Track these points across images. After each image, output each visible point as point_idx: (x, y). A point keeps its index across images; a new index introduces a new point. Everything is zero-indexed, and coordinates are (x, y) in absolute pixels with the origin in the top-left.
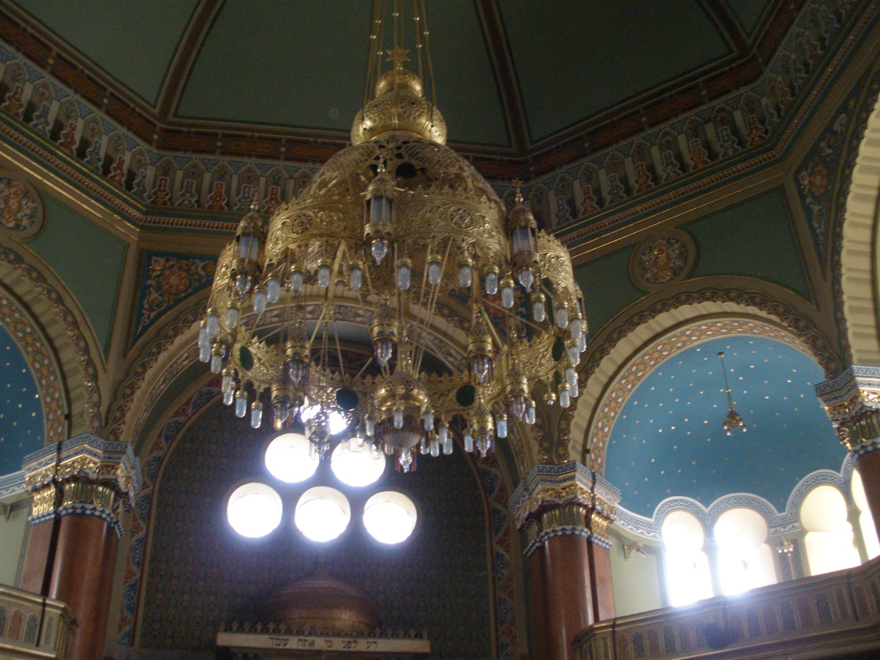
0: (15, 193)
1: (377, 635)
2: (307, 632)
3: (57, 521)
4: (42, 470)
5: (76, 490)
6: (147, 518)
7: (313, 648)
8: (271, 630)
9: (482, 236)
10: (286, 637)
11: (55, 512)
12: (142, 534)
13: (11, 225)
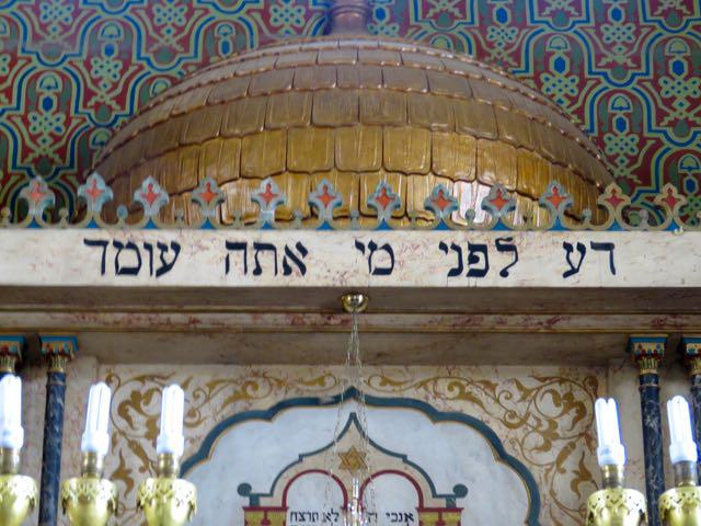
1: (615, 213)
7: (295, 280)
8: (94, 208)
10: (168, 236)
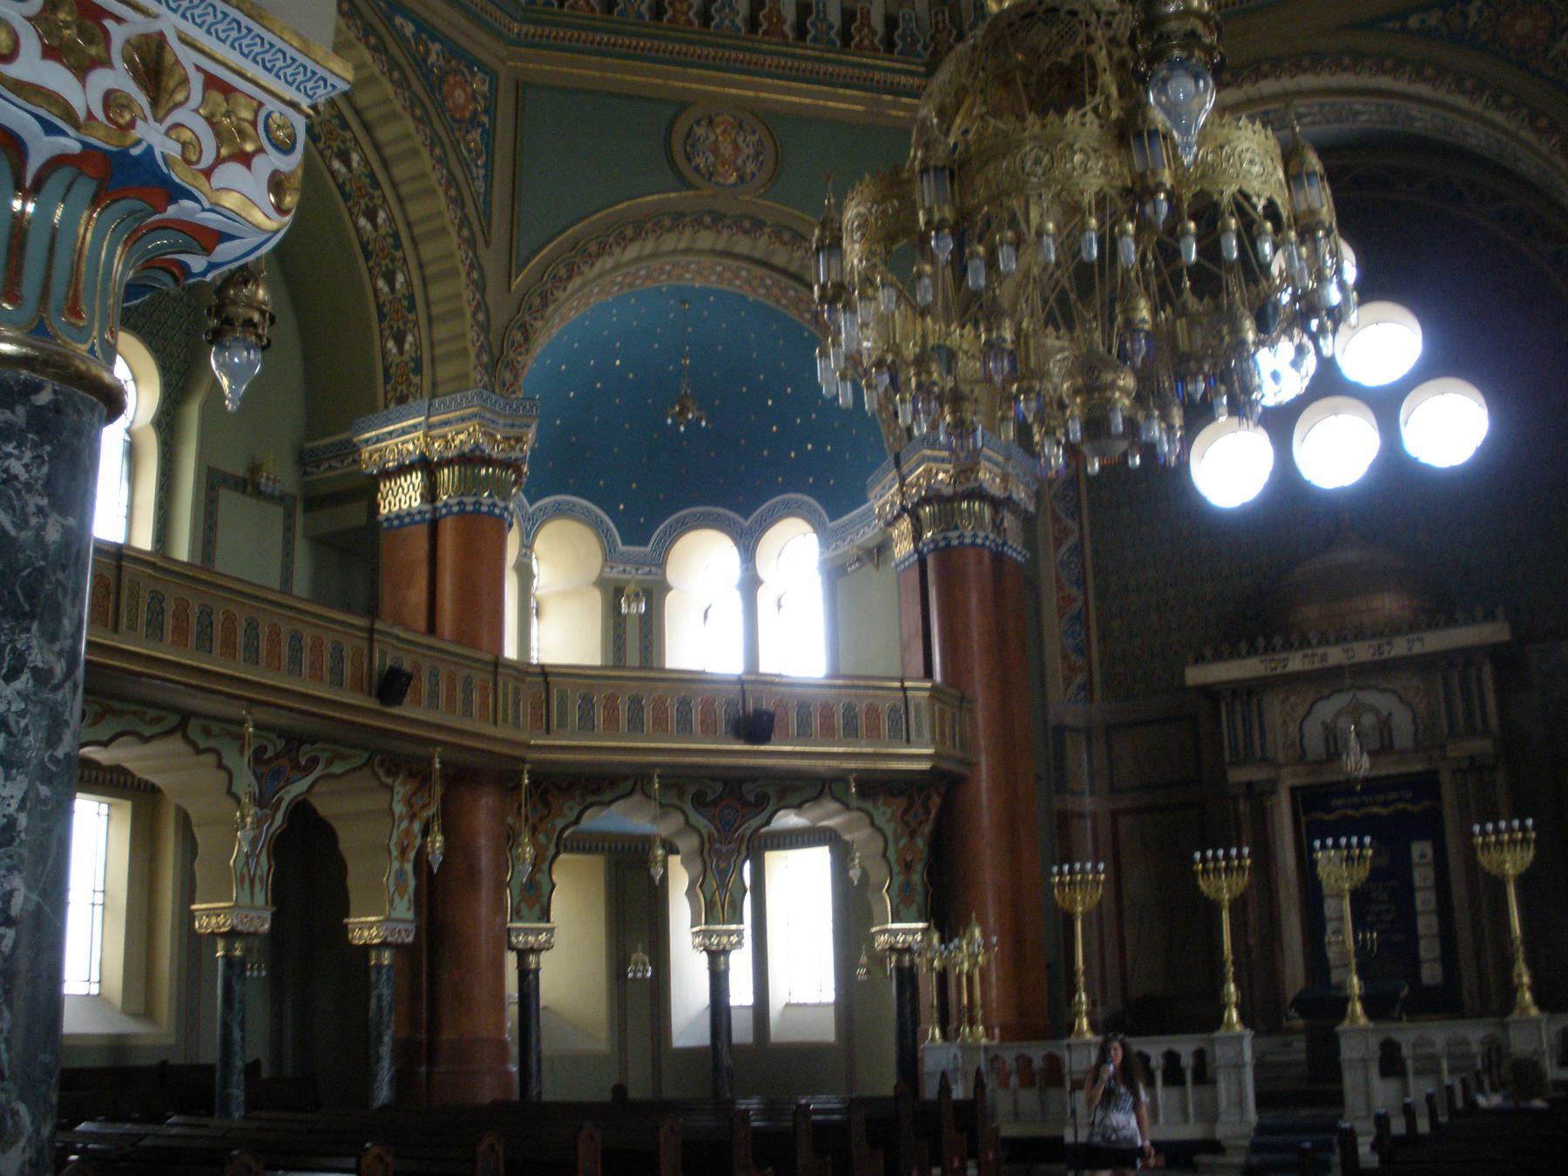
0: (724, 132)
2: (1315, 642)
3: (922, 563)
4: (888, 496)
5: (933, 515)
6: (1076, 513)
9: (1069, 177)
11: (916, 550)
12: (1072, 540)
13: (733, 178)
